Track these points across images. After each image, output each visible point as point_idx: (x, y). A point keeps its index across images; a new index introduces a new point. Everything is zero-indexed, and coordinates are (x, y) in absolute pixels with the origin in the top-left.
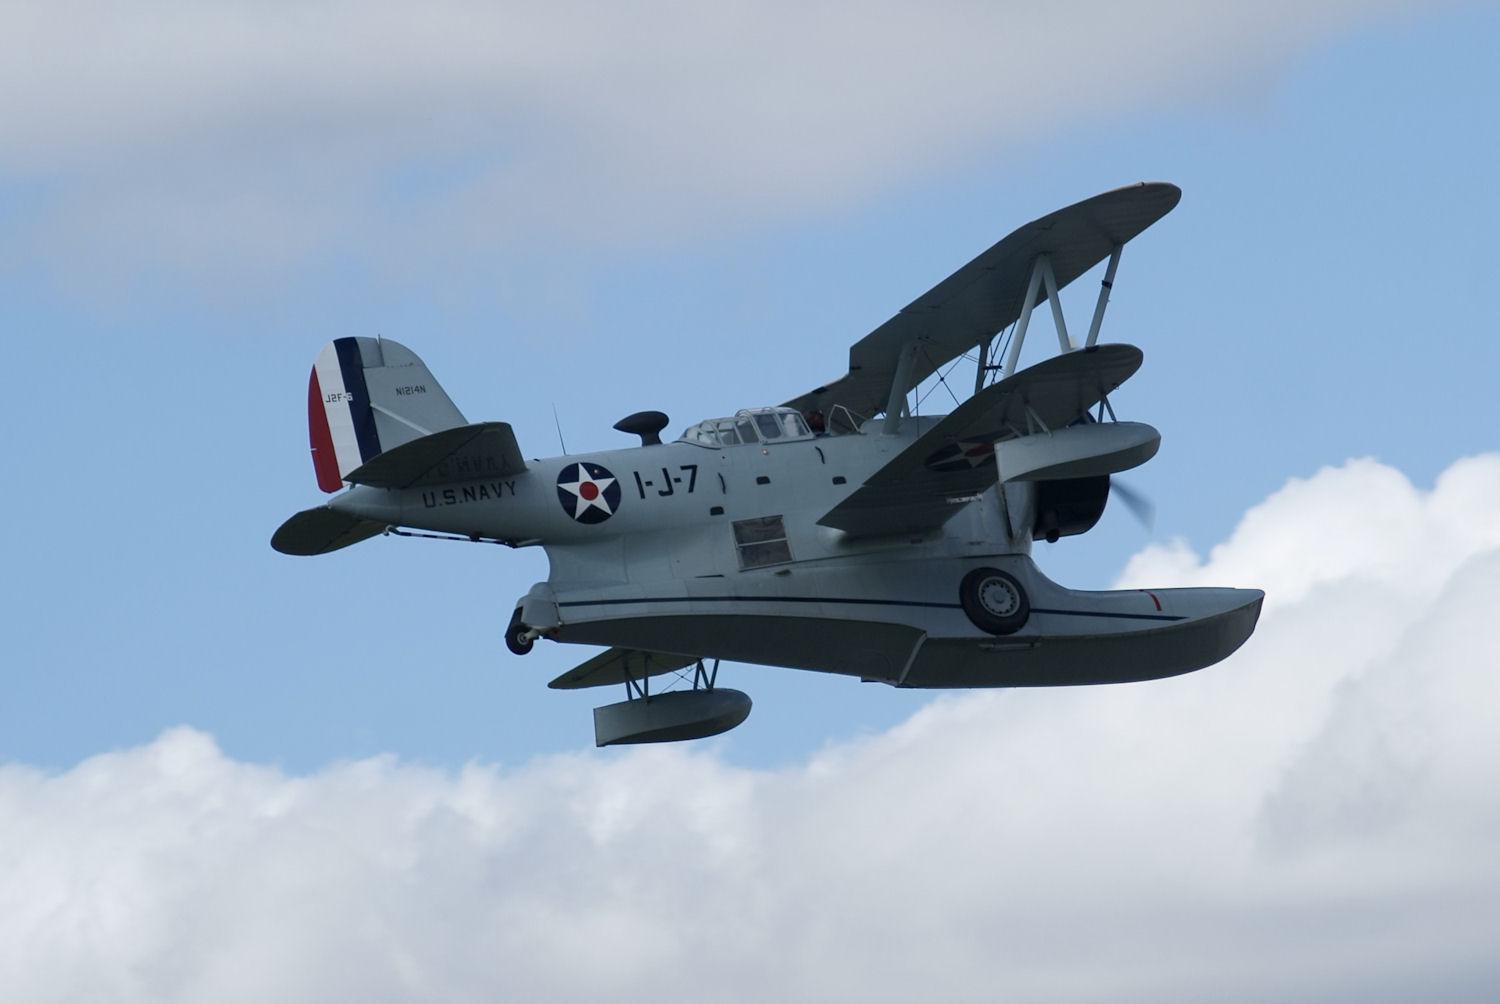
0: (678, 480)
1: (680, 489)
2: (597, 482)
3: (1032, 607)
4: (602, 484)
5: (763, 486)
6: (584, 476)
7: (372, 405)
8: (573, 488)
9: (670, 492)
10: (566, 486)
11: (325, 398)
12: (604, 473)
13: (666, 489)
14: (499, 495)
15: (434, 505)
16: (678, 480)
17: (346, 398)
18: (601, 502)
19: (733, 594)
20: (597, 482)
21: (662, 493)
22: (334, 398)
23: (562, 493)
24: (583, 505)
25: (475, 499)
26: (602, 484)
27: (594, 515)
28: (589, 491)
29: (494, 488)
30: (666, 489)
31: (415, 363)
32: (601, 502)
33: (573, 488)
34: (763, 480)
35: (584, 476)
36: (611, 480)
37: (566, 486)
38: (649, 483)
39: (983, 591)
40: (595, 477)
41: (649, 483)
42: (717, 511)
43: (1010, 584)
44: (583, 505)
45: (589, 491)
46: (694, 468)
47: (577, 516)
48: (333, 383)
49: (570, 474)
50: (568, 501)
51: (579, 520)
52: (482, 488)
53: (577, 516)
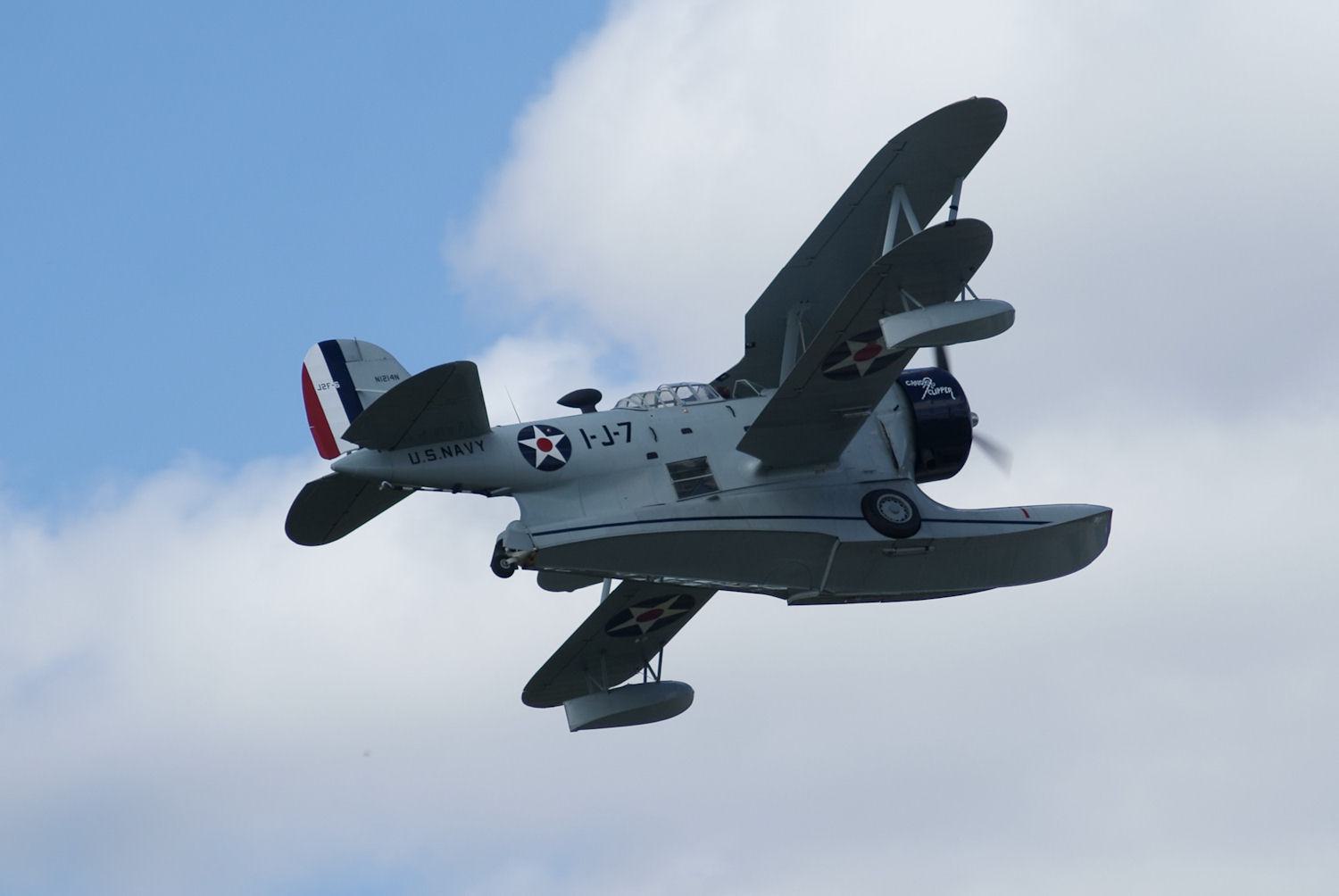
0: (616, 434)
1: (620, 440)
3: (923, 517)
4: (555, 439)
5: (687, 435)
9: (612, 442)
10: (525, 442)
12: (555, 431)
13: (608, 440)
14: (471, 452)
15: (419, 462)
16: (616, 434)
18: (555, 453)
21: (605, 444)
23: (523, 448)
24: (541, 456)
25: (451, 455)
26: (555, 439)
27: (551, 464)
28: (545, 445)
30: (608, 440)
32: (555, 453)
33: (531, 443)
34: (686, 431)
37: (525, 442)
38: (593, 437)
39: (881, 506)
41: (593, 437)
42: (652, 456)
43: (903, 500)
44: (541, 456)
45: (545, 445)
46: (629, 424)
50: (529, 454)
53: (537, 466)
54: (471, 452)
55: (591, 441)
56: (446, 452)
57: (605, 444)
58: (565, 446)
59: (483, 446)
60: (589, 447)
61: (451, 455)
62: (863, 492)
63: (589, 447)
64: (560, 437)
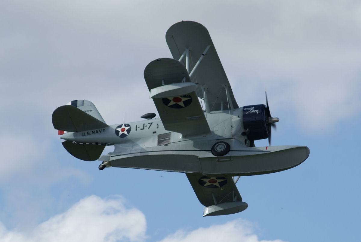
4: (127, 128)
8: (119, 129)
14: (100, 132)
18: (125, 132)
21: (141, 129)
24: (121, 133)
25: (94, 133)
26: (127, 128)
27: (123, 136)
28: (123, 130)
32: (125, 132)
33: (119, 129)
35: (123, 127)
36: (128, 127)
44: (121, 133)
47: (119, 136)
50: (117, 132)
52: (97, 131)
54: (100, 132)
55: (137, 128)
56: (93, 133)
57: (141, 129)
58: (129, 131)
59: (105, 131)
60: (136, 130)
61: (94, 133)
62: (215, 142)
63: (136, 130)
64: (128, 127)
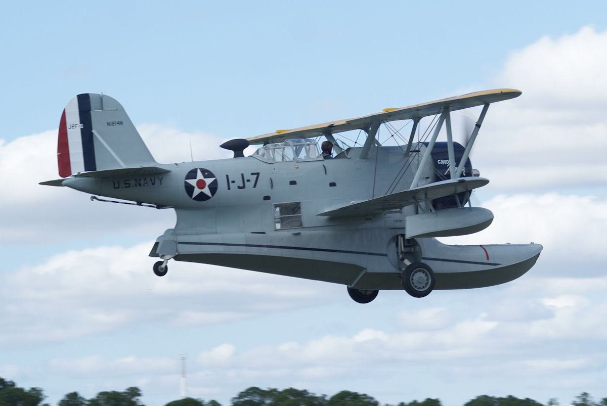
0: (248, 181)
1: (249, 185)
2: (206, 180)
4: (209, 181)
6: (200, 176)
7: (93, 131)
9: (243, 187)
11: (68, 126)
13: (241, 185)
14: (153, 184)
15: (118, 188)
16: (248, 181)
17: (79, 127)
18: (206, 191)
19: (269, 244)
20: (206, 180)
21: (239, 188)
22: (73, 126)
24: (197, 191)
26: (209, 181)
27: (202, 197)
28: (201, 184)
29: (151, 180)
31: (119, 109)
32: (206, 191)
33: (193, 182)
34: (293, 183)
35: (200, 176)
38: (233, 182)
40: (205, 177)
41: (233, 182)
44: (197, 191)
46: (258, 174)
48: (74, 118)
49: (192, 174)
50: (189, 189)
51: (194, 199)
